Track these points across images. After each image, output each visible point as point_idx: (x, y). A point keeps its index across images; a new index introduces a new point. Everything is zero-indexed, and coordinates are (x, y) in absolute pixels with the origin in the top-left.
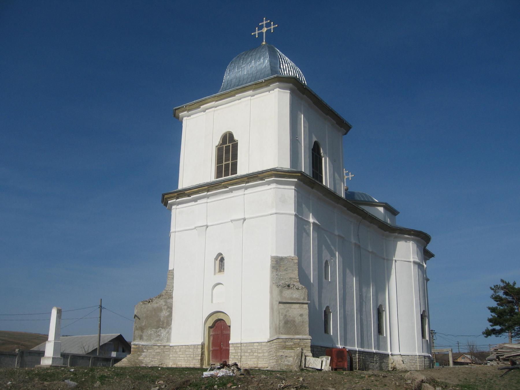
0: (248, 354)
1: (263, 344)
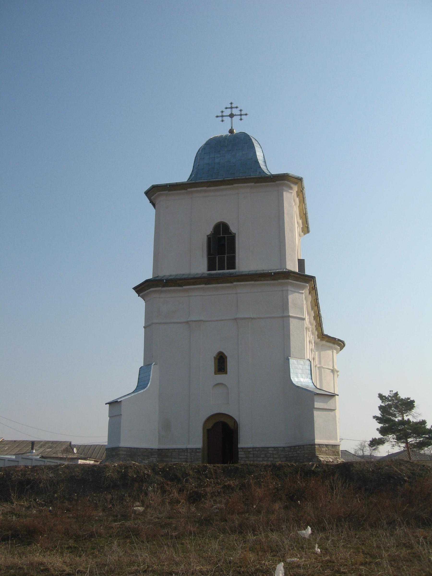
0: (261, 459)
1: (280, 449)
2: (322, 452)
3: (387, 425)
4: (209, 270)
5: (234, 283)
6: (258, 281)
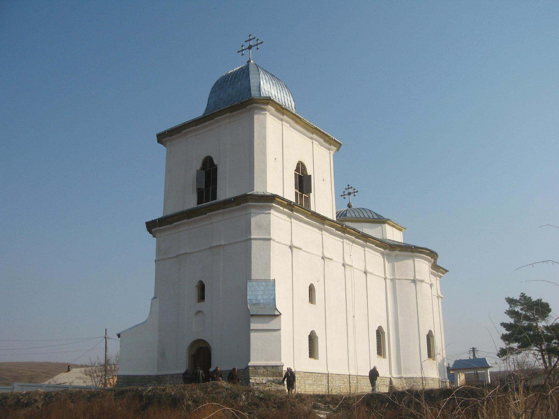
1: (241, 371)
2: (257, 374)
3: (508, 332)
4: (198, 203)
5: (208, 214)
6: (226, 208)
